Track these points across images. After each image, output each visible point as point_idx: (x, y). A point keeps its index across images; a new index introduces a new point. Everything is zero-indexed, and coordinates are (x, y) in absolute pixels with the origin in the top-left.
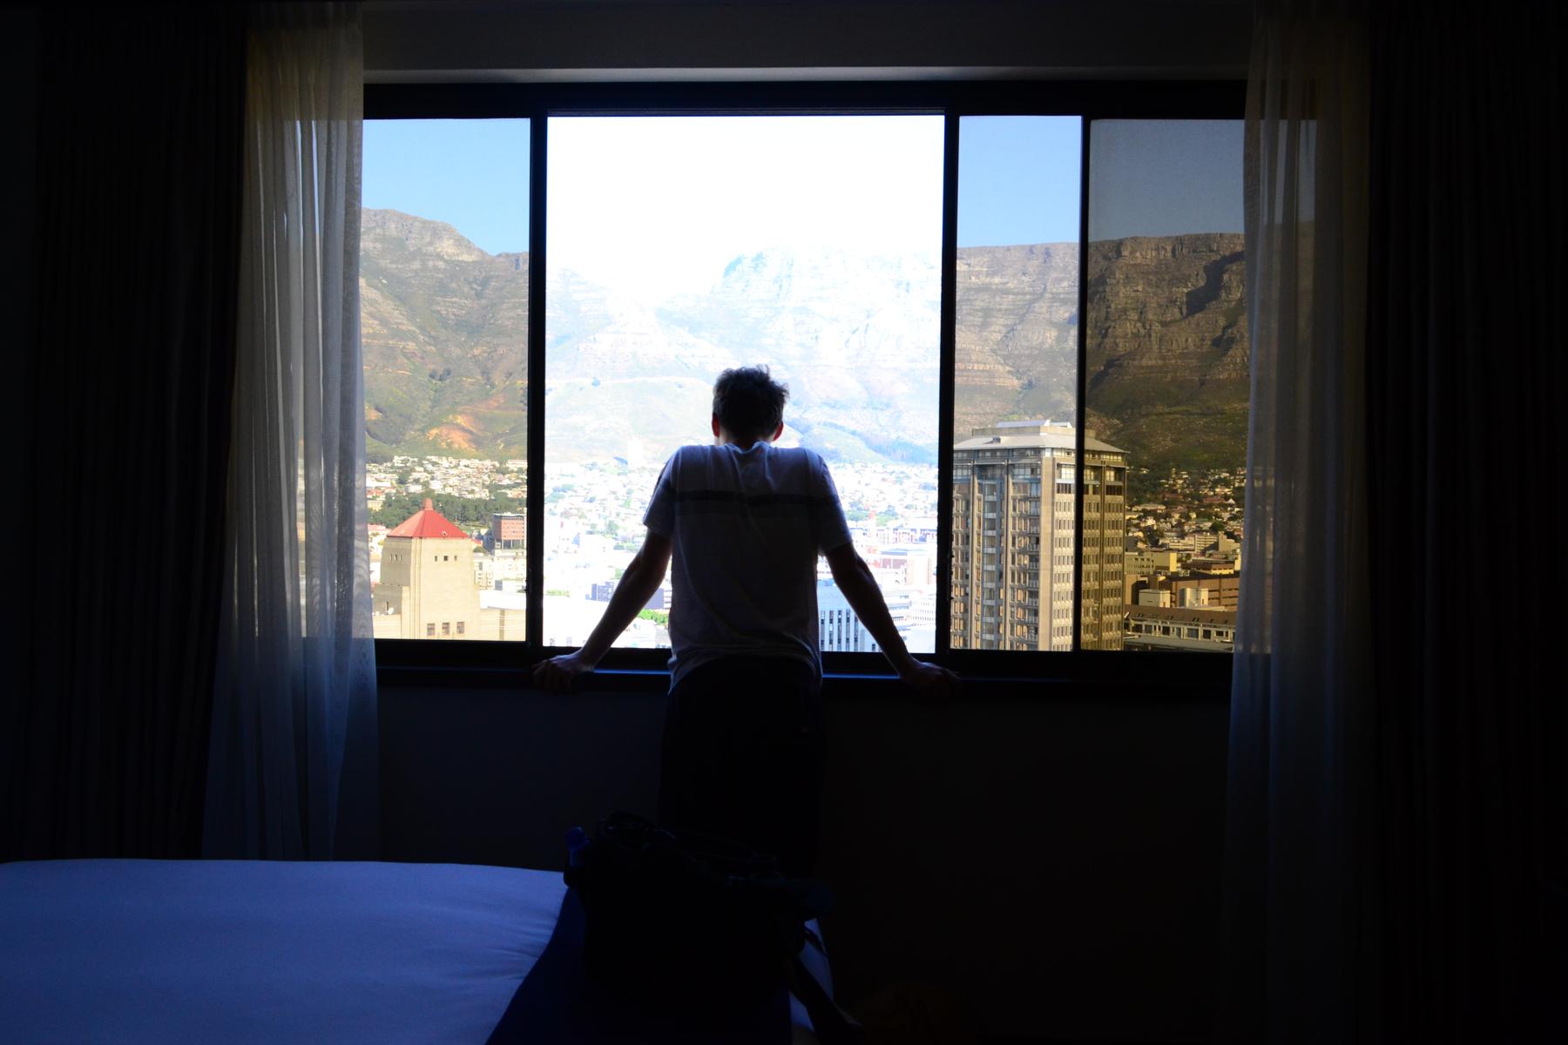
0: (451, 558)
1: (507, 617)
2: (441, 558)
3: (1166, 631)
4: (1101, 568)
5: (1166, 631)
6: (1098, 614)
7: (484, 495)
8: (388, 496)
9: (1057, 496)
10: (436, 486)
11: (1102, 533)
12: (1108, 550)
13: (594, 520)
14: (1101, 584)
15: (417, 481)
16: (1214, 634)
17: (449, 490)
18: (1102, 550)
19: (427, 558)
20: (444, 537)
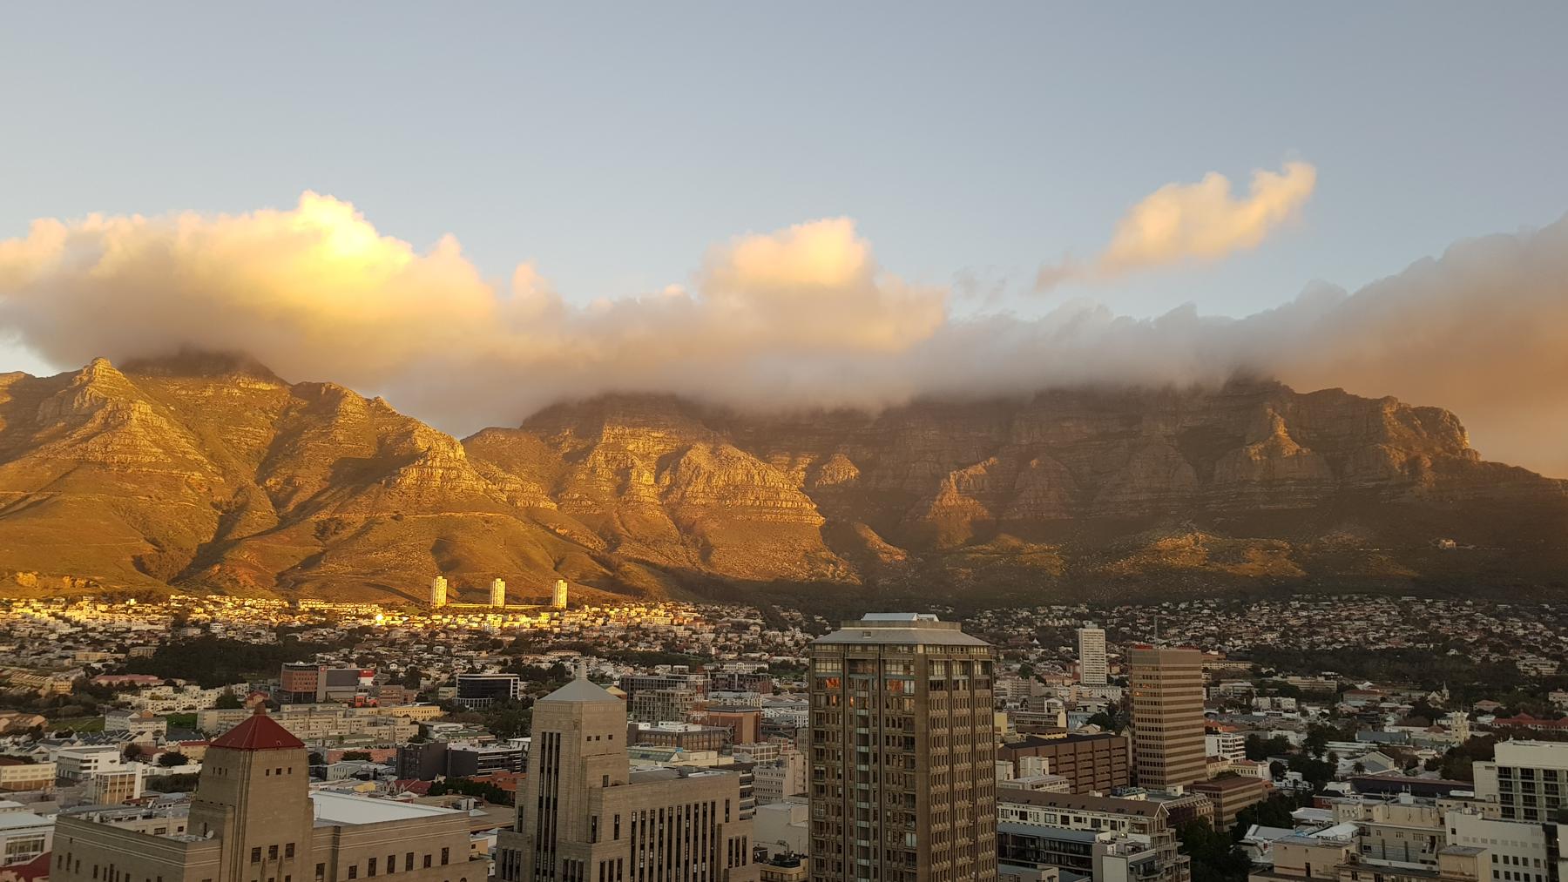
0: (285, 772)
1: (343, 835)
2: (273, 772)
3: (1023, 816)
4: (974, 766)
5: (1023, 816)
6: (973, 815)
7: (268, 638)
8: (162, 640)
9: (931, 694)
10: (216, 629)
11: (973, 729)
12: (979, 747)
13: (393, 667)
14: (974, 783)
15: (196, 624)
16: (1071, 820)
17: (231, 634)
18: (974, 747)
19: (257, 772)
20: (278, 748)
